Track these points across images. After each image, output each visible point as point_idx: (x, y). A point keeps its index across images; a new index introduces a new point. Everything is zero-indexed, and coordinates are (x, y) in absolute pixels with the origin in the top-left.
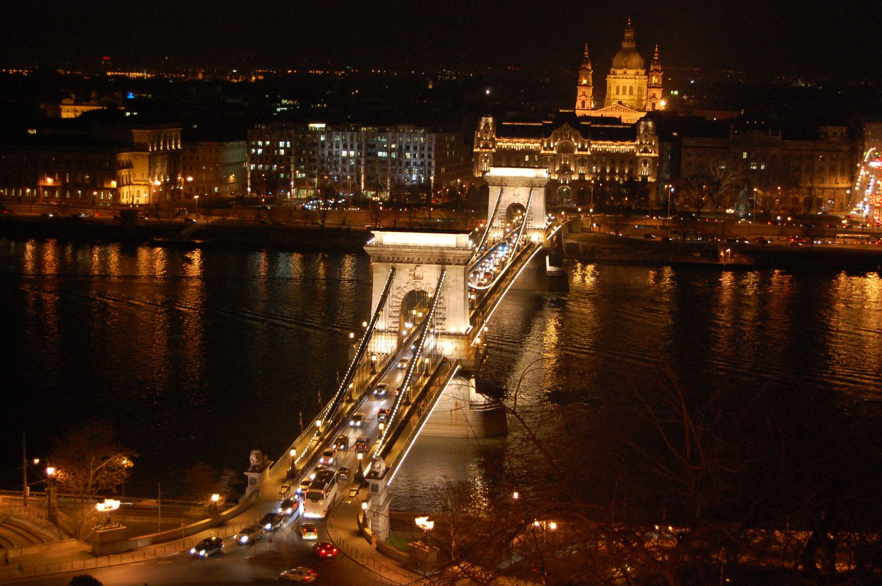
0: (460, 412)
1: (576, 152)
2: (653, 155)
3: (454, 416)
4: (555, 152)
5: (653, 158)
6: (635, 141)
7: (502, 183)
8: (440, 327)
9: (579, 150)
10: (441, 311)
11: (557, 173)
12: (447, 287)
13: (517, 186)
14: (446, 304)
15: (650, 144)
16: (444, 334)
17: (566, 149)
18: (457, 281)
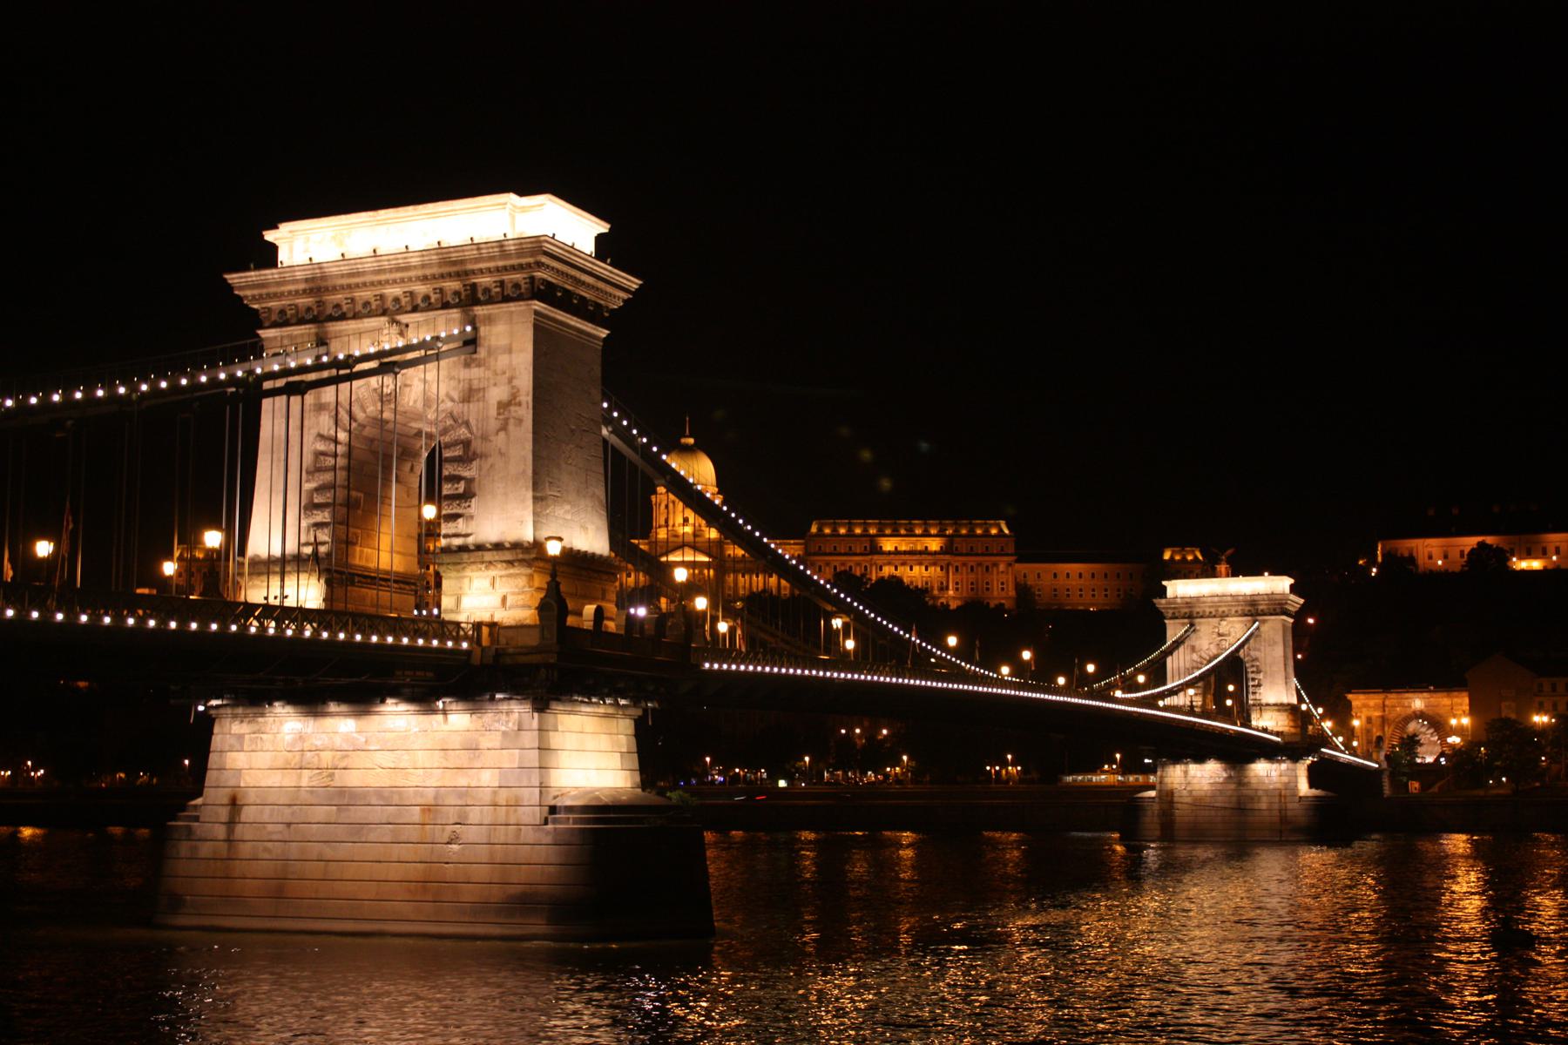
7: (1191, 613)
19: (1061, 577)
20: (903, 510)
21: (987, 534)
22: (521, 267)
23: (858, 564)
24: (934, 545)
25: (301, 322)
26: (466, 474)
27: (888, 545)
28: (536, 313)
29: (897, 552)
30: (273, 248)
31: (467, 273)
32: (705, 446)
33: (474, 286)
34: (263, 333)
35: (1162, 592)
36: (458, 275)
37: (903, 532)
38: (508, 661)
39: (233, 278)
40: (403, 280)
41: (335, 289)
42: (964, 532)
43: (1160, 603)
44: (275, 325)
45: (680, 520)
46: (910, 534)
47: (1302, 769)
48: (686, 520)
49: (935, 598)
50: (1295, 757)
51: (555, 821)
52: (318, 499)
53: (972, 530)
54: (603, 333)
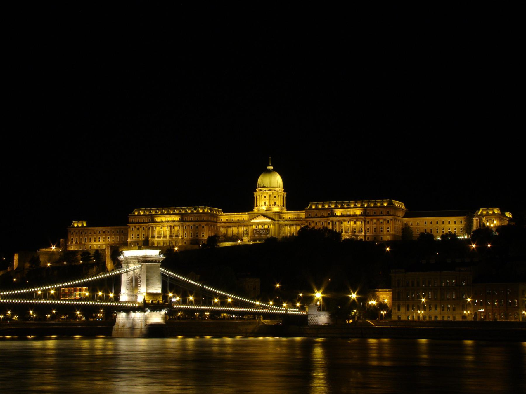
7: (127, 262)
19: (428, 224)
20: (344, 196)
21: (382, 206)
23: (326, 221)
24: (358, 212)
27: (338, 212)
29: (342, 215)
32: (277, 170)
37: (346, 206)
42: (372, 205)
45: (263, 204)
46: (349, 207)
48: (265, 203)
49: (357, 236)
53: (375, 205)
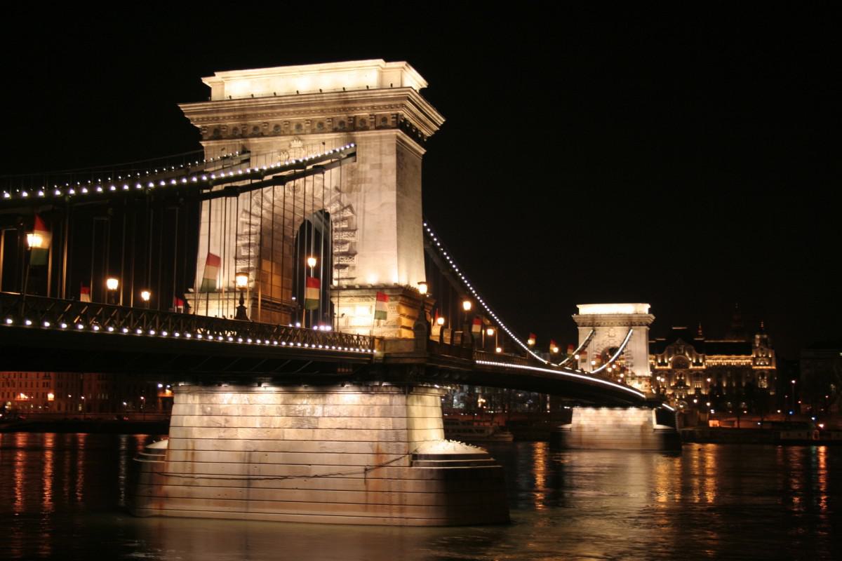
0: (384, 472)
1: (691, 367)
2: (769, 367)
3: (372, 483)
4: (669, 367)
5: (770, 371)
6: (750, 354)
7: (594, 322)
8: (344, 273)
9: (694, 365)
10: (344, 236)
11: (672, 388)
12: (360, 181)
13: (612, 325)
14: (358, 221)
15: (767, 356)
16: (350, 288)
17: (680, 364)
18: (380, 165)
22: (391, 107)
25: (234, 137)
26: (352, 239)
28: (398, 137)
30: (208, 90)
31: (350, 108)
33: (355, 117)
34: (204, 144)
35: (577, 311)
36: (344, 109)
38: (392, 361)
39: (184, 107)
40: (305, 111)
41: (255, 116)
43: (574, 316)
44: (210, 139)
47: (653, 414)
50: (651, 407)
51: (418, 464)
52: (244, 253)
54: (423, 151)
